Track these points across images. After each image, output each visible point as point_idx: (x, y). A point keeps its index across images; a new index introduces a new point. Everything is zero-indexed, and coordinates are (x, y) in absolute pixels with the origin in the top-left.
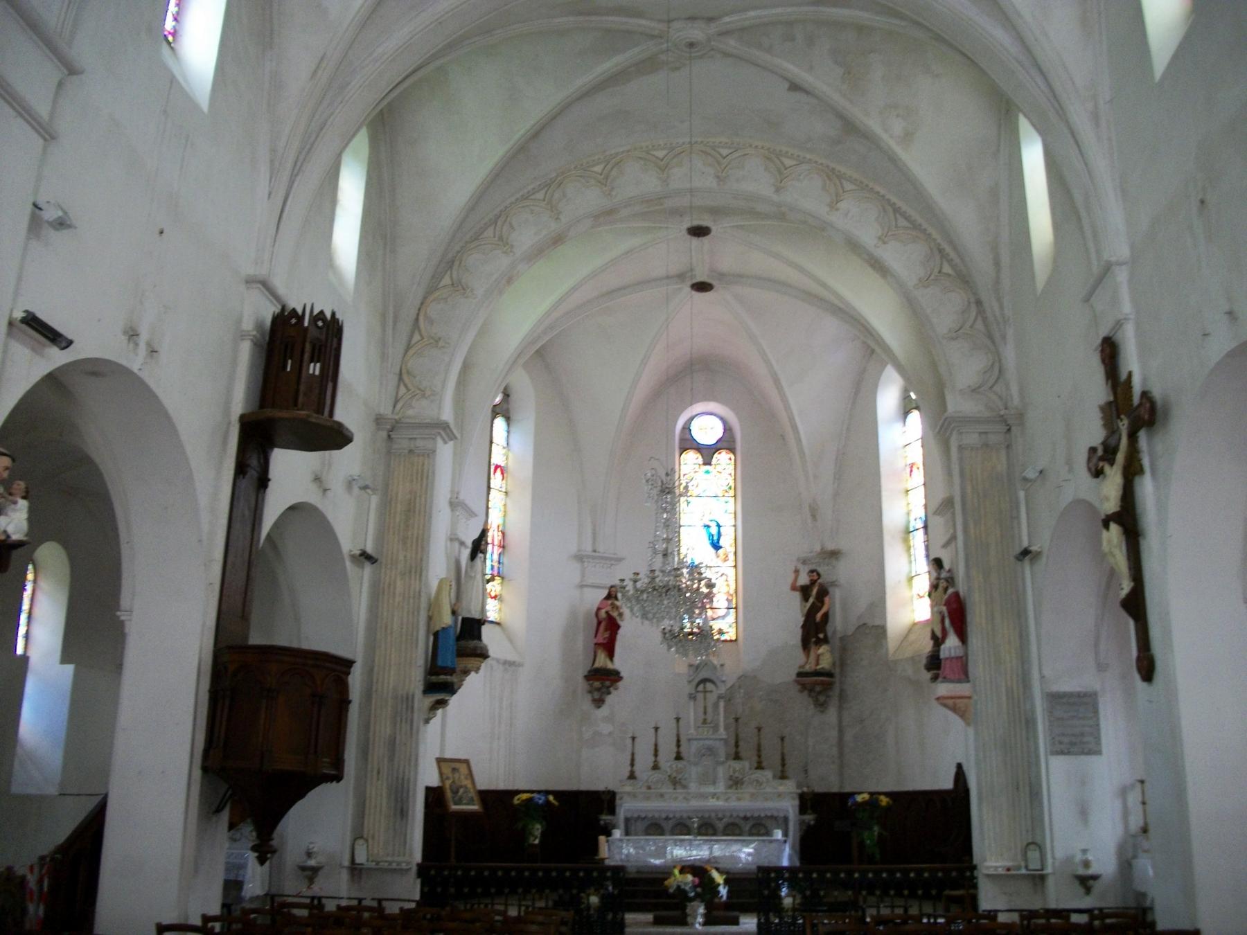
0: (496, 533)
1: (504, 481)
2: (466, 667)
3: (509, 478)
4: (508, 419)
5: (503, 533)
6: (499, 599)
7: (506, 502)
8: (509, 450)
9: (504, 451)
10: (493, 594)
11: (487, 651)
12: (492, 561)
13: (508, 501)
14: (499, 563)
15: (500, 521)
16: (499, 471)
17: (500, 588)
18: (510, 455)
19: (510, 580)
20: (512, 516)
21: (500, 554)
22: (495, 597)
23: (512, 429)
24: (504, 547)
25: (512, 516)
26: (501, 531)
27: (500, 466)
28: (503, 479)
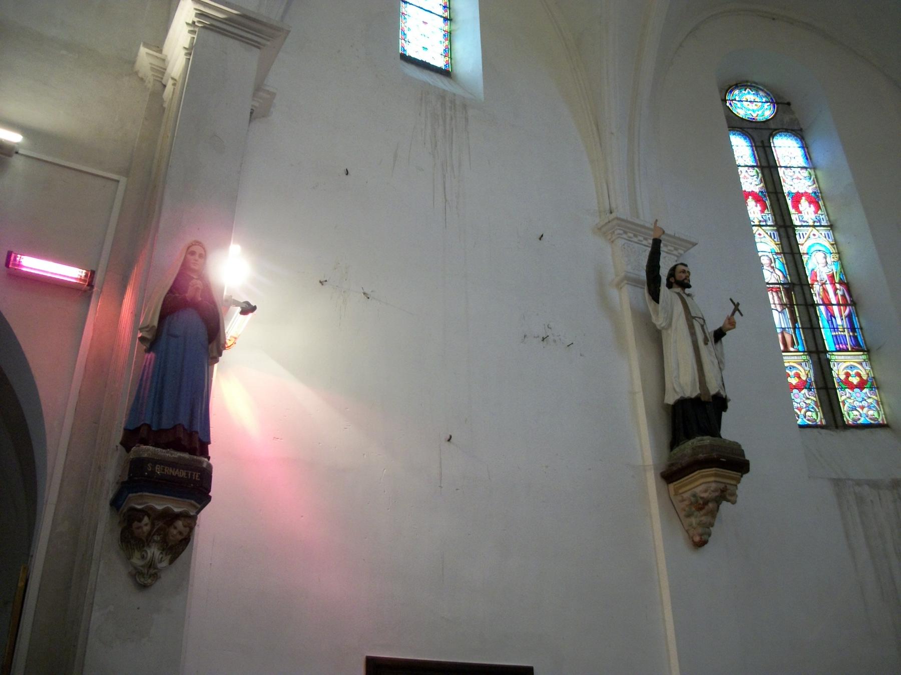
0: (829, 288)
1: (820, 212)
2: (694, 496)
3: (828, 204)
4: (798, 133)
5: (846, 284)
6: (871, 388)
7: (835, 240)
8: (814, 168)
9: (805, 173)
10: (855, 380)
11: (742, 453)
12: (834, 328)
13: (840, 238)
14: (852, 328)
15: (834, 268)
16: (804, 204)
17: (868, 368)
18: (819, 173)
19: (879, 348)
20: (849, 252)
21: (849, 317)
22: (861, 385)
23: (809, 140)
24: (854, 304)
25: (849, 252)
26: (841, 283)
27: (802, 195)
28: (818, 208)
